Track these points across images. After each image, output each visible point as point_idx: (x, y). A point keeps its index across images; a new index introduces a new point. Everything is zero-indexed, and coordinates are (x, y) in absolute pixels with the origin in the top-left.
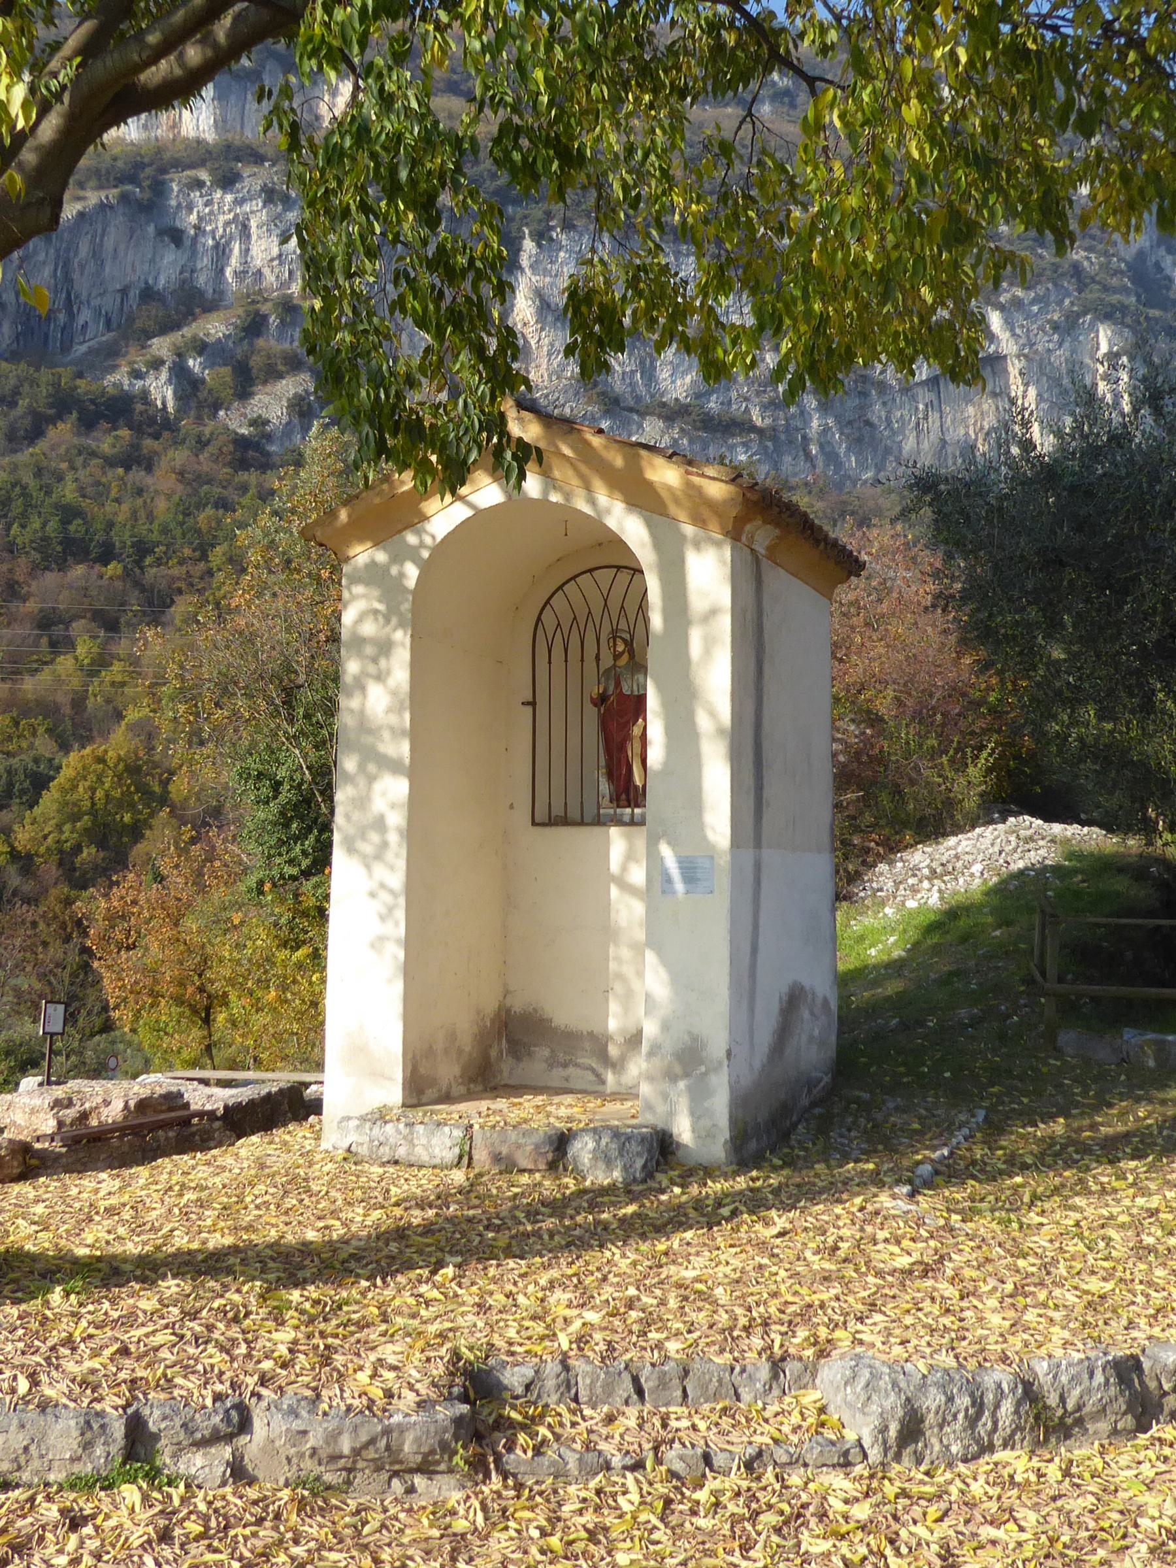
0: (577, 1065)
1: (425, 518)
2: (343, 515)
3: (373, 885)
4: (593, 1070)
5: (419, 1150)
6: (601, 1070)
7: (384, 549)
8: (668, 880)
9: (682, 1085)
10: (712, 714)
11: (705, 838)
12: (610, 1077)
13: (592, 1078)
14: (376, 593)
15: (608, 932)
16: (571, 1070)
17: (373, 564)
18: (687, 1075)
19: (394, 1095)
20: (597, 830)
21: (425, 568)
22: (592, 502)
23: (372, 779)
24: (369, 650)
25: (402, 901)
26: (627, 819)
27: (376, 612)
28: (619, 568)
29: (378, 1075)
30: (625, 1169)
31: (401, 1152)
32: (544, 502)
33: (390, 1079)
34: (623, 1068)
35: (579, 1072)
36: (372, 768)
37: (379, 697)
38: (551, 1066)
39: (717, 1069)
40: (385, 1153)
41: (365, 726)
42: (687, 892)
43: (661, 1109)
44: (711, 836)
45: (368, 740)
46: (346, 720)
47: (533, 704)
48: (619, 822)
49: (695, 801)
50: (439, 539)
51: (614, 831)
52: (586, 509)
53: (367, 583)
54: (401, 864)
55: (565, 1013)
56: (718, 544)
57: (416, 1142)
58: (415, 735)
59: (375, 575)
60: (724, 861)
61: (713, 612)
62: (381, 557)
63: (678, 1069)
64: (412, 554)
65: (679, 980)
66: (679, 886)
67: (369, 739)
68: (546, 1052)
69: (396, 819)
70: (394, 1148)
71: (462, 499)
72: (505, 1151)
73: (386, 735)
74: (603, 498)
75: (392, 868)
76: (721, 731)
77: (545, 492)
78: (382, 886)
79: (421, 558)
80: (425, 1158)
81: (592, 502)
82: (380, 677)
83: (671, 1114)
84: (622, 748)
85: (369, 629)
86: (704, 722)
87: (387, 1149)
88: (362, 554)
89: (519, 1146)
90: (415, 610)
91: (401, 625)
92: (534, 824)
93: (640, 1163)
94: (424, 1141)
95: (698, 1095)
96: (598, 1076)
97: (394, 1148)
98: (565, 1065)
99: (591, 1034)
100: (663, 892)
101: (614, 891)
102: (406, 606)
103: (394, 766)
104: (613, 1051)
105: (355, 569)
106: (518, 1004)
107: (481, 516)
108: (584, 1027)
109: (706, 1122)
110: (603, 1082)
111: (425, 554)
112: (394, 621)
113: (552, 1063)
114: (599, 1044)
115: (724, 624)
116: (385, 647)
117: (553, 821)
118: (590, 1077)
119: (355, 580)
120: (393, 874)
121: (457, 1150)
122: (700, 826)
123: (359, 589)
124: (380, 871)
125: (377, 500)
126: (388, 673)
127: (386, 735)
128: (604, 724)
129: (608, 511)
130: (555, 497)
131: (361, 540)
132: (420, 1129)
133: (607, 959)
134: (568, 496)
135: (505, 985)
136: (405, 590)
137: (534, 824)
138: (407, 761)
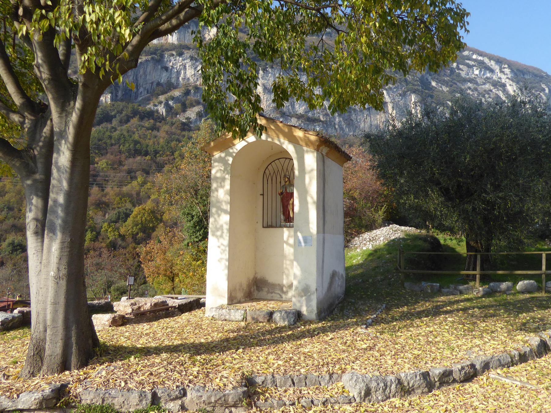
0: (275, 293)
1: (234, 145)
2: (212, 144)
3: (219, 244)
5: (232, 317)
6: (281, 294)
8: (300, 242)
9: (304, 298)
10: (312, 198)
11: (310, 231)
12: (284, 296)
13: (279, 296)
14: (221, 165)
15: (283, 256)
16: (273, 294)
17: (220, 157)
18: (305, 295)
19: (225, 301)
20: (280, 229)
21: (234, 158)
22: (280, 141)
23: (219, 216)
24: (219, 181)
25: (227, 249)
26: (288, 226)
27: (221, 170)
28: (286, 158)
29: (221, 296)
30: (288, 321)
31: (227, 317)
32: (266, 141)
35: (276, 295)
36: (219, 212)
37: (221, 193)
38: (268, 293)
39: (313, 294)
41: (219, 201)
44: (311, 230)
45: (219, 204)
46: (212, 199)
47: (263, 195)
48: (286, 227)
49: (307, 222)
50: (239, 150)
51: (285, 229)
52: (278, 143)
54: (227, 238)
55: (271, 279)
56: (312, 152)
58: (231, 203)
60: (315, 237)
61: (312, 170)
62: (223, 155)
63: (303, 294)
64: (230, 155)
65: (303, 270)
66: (303, 244)
68: (266, 289)
69: (226, 227)
70: (225, 316)
71: (244, 140)
72: (255, 317)
73: (224, 204)
74: (282, 140)
75: (224, 239)
76: (314, 202)
77: (267, 138)
78: (222, 244)
80: (234, 319)
81: (280, 141)
83: (301, 306)
84: (287, 207)
85: (219, 175)
86: (309, 200)
88: (217, 155)
89: (260, 315)
90: (231, 169)
91: (228, 173)
92: (263, 227)
93: (292, 320)
94: (233, 314)
95: (308, 300)
96: (281, 296)
97: (225, 316)
98: (272, 293)
99: (279, 285)
101: (285, 245)
102: (229, 168)
103: (225, 212)
104: (285, 289)
105: (216, 159)
106: (259, 276)
108: (277, 283)
109: (310, 309)
110: (282, 298)
111: (234, 154)
112: (226, 172)
113: (268, 292)
114: (281, 287)
115: (315, 173)
116: (224, 179)
117: (269, 226)
118: (279, 296)
119: (216, 161)
120: (225, 241)
121: (242, 317)
123: (216, 164)
124: (221, 240)
125: (221, 140)
126: (224, 186)
127: (224, 204)
128: (282, 200)
129: (284, 143)
130: (269, 140)
131: (217, 151)
132: (232, 311)
133: (283, 264)
134: (273, 139)
135: (255, 271)
137: (263, 227)
138: (229, 210)
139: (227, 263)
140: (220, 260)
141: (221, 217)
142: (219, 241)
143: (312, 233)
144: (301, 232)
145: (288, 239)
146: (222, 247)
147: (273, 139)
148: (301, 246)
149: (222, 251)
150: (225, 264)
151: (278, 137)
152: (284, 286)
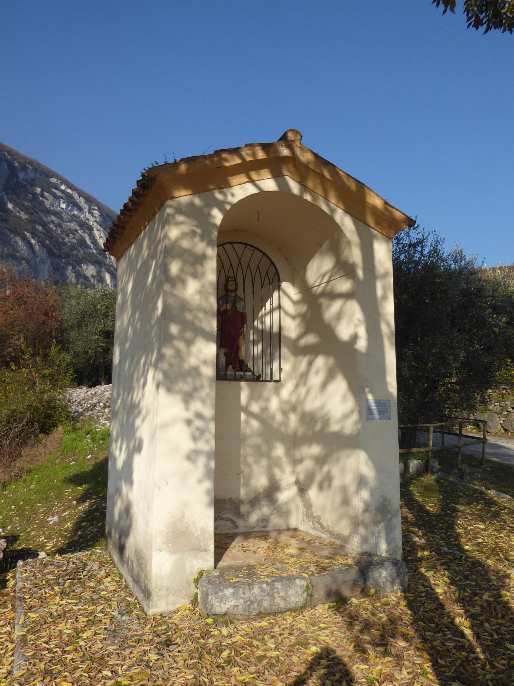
3: (190, 415)
4: (231, 521)
5: (278, 600)
6: (236, 520)
7: (199, 197)
8: (370, 411)
12: (241, 523)
17: (191, 204)
19: (207, 561)
20: (233, 383)
22: (328, 205)
23: (189, 343)
25: (212, 426)
32: (300, 198)
33: (206, 551)
34: (248, 517)
35: (224, 523)
36: (189, 335)
40: (255, 609)
42: (380, 419)
43: (372, 541)
51: (243, 384)
52: (324, 208)
53: (101, 215)
57: (276, 595)
59: (190, 211)
62: (197, 201)
66: (377, 416)
67: (189, 317)
71: (252, 181)
78: (199, 416)
79: (225, 209)
80: (282, 604)
82: (195, 276)
87: (255, 605)
88: (184, 196)
93: (407, 578)
94: (282, 594)
96: (234, 523)
99: (230, 499)
100: (368, 419)
101: (243, 416)
103: (207, 336)
104: (244, 509)
105: (179, 204)
107: (262, 194)
110: (237, 527)
111: (228, 207)
116: (202, 258)
119: (179, 210)
121: (305, 595)
122: (385, 384)
124: (196, 406)
130: (308, 197)
132: (278, 585)
136: (214, 225)
139: (213, 464)
140: (191, 457)
141: (194, 349)
142: (187, 409)
143: (391, 394)
144: (372, 392)
145: (249, 403)
146: (198, 423)
147: (315, 198)
148: (374, 419)
149: (197, 434)
150: (207, 466)
151: (326, 199)
152: (241, 502)
